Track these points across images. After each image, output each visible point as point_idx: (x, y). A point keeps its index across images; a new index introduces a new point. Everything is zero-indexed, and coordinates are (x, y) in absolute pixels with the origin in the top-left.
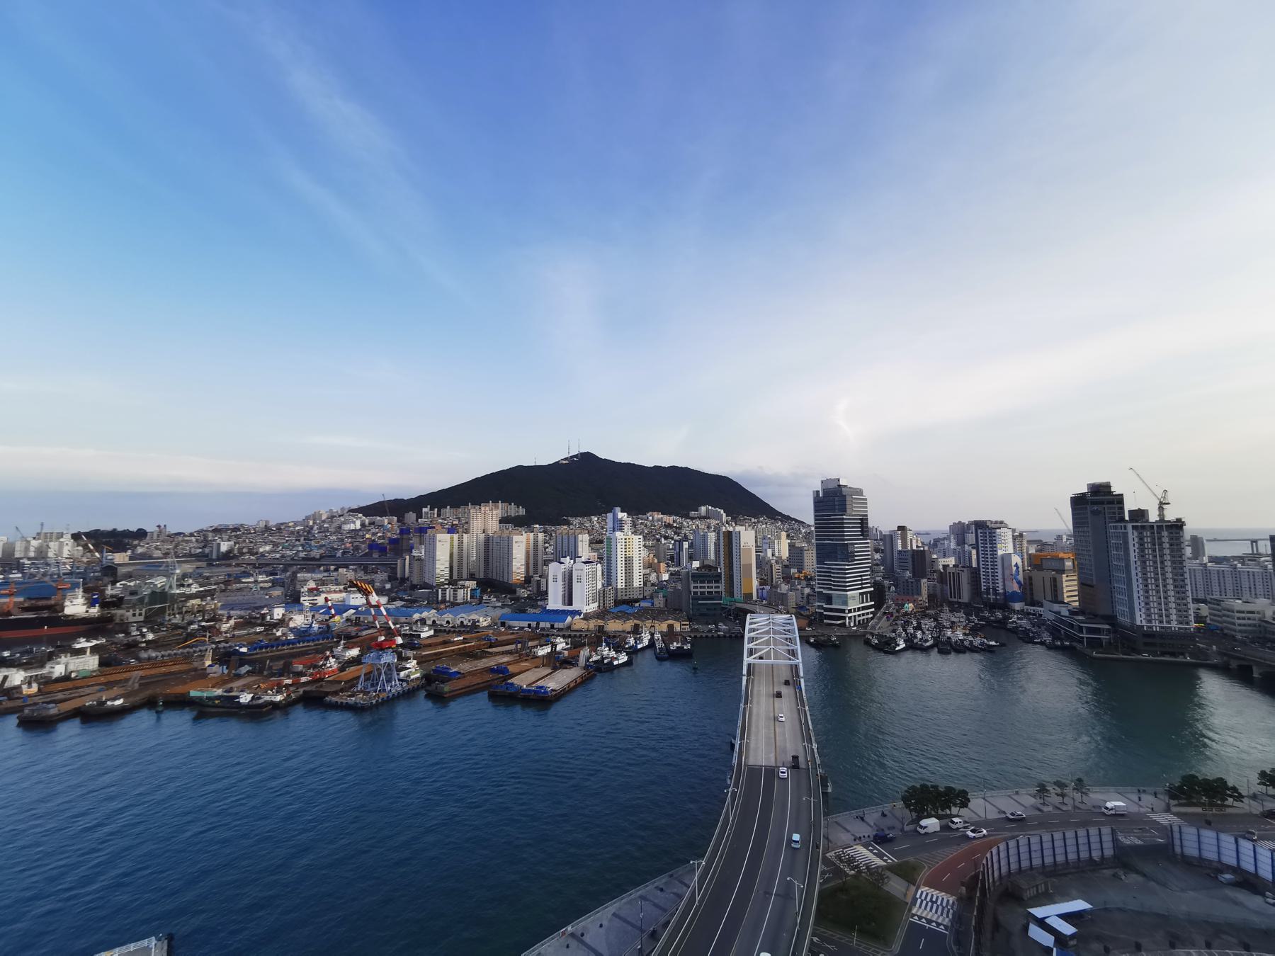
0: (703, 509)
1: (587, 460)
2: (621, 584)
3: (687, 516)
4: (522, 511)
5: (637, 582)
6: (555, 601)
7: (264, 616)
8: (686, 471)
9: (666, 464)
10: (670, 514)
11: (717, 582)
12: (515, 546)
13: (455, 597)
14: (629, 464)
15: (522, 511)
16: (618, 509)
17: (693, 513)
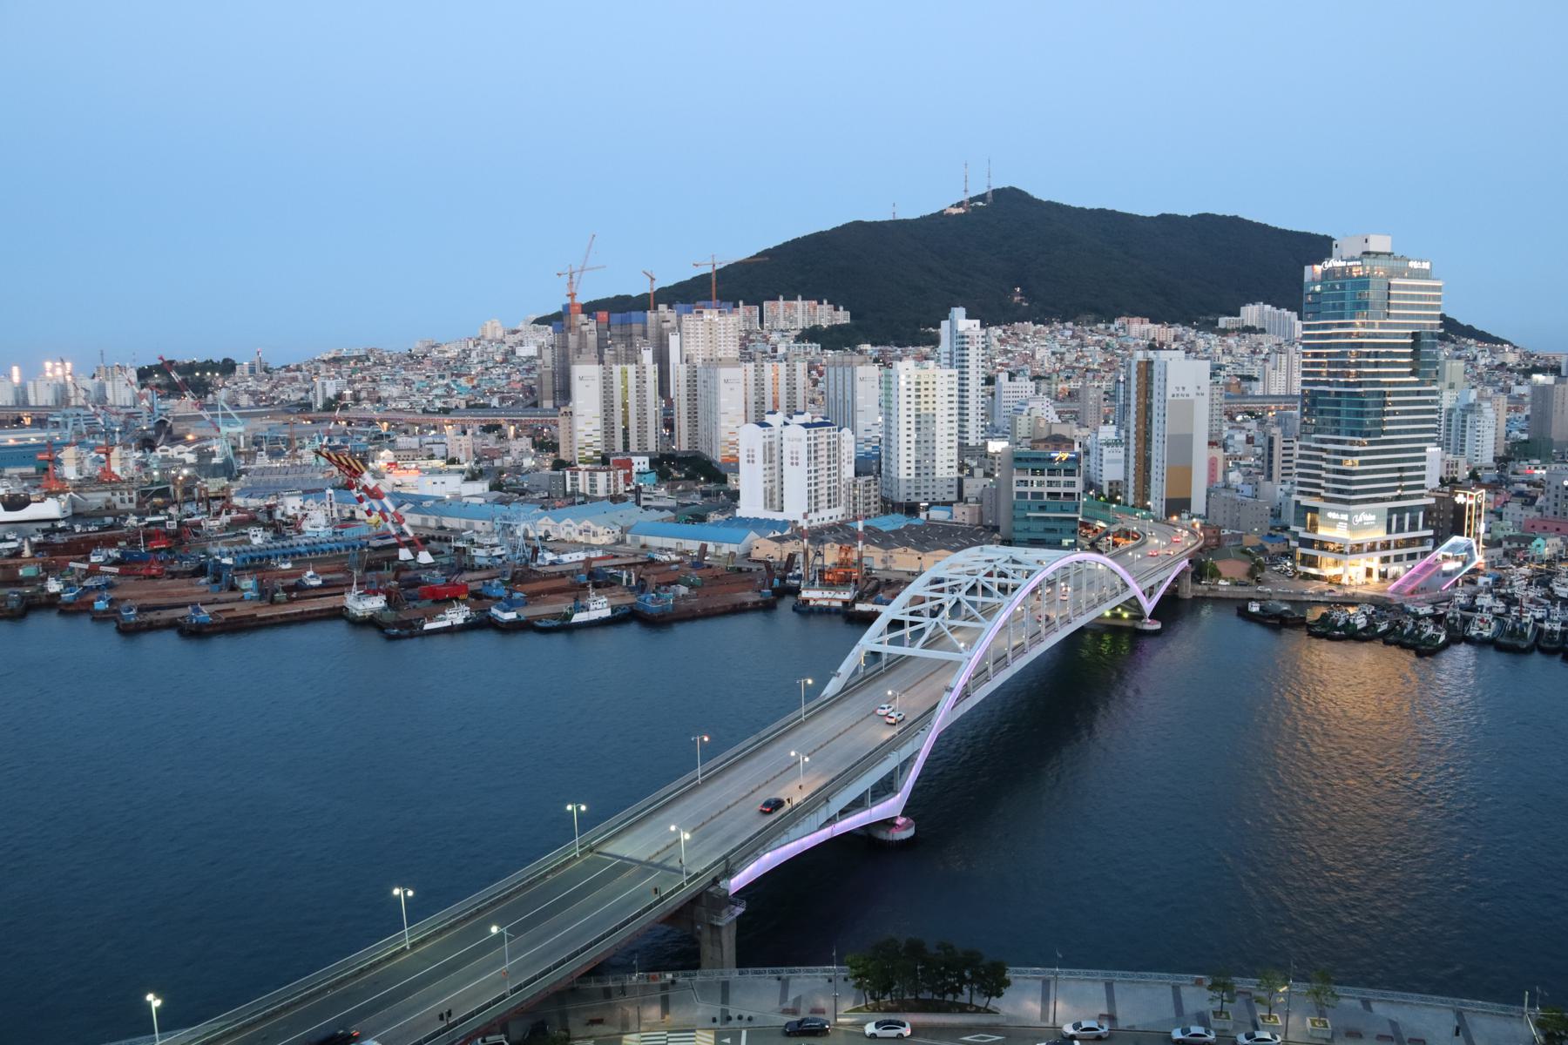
0: (1252, 313)
1: (1009, 200)
2: (903, 467)
3: (1211, 327)
4: (843, 317)
5: (945, 465)
6: (751, 505)
7: (270, 510)
8: (1235, 220)
9: (1188, 210)
10: (1172, 322)
11: (1070, 472)
12: (724, 389)
13: (593, 485)
14: (1102, 211)
15: (843, 317)
16: (959, 313)
17: (1223, 322)
